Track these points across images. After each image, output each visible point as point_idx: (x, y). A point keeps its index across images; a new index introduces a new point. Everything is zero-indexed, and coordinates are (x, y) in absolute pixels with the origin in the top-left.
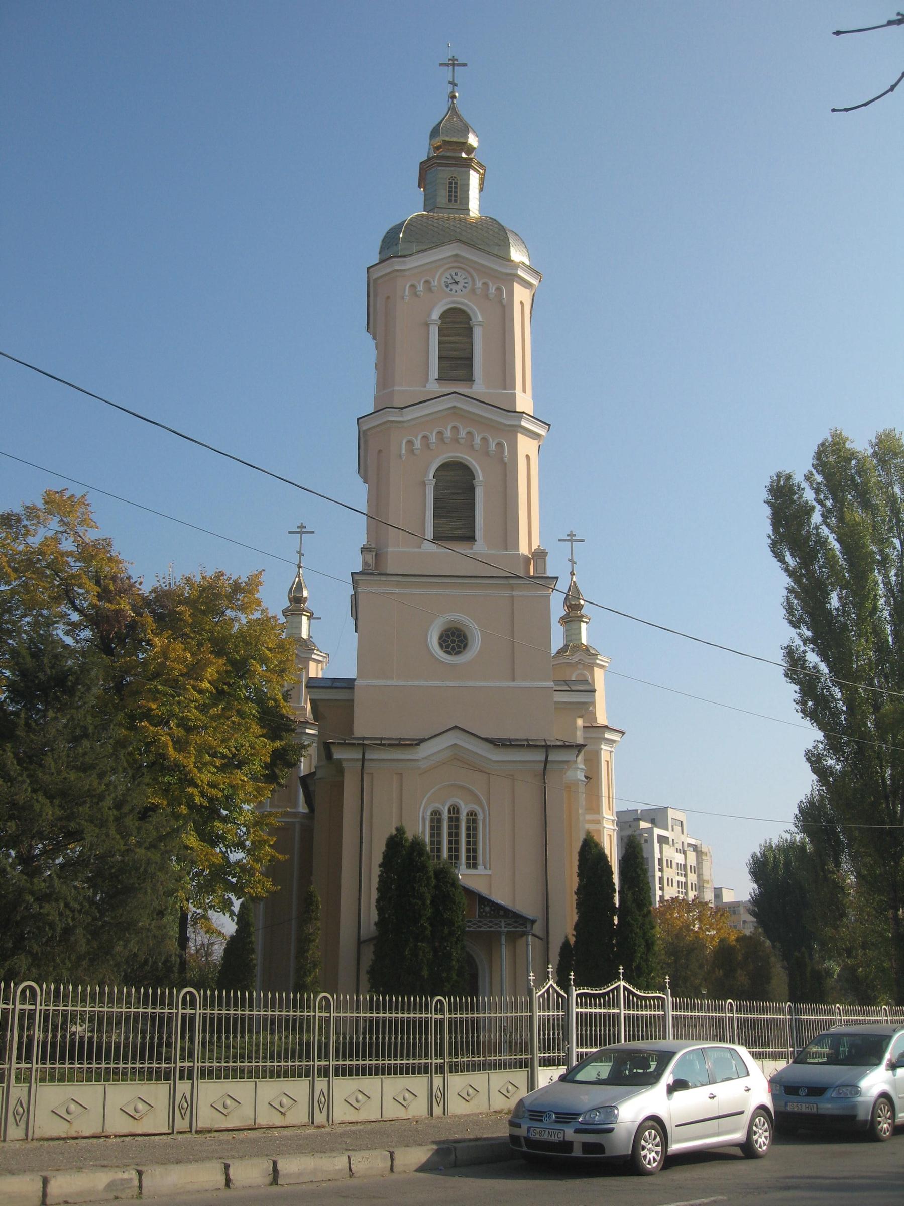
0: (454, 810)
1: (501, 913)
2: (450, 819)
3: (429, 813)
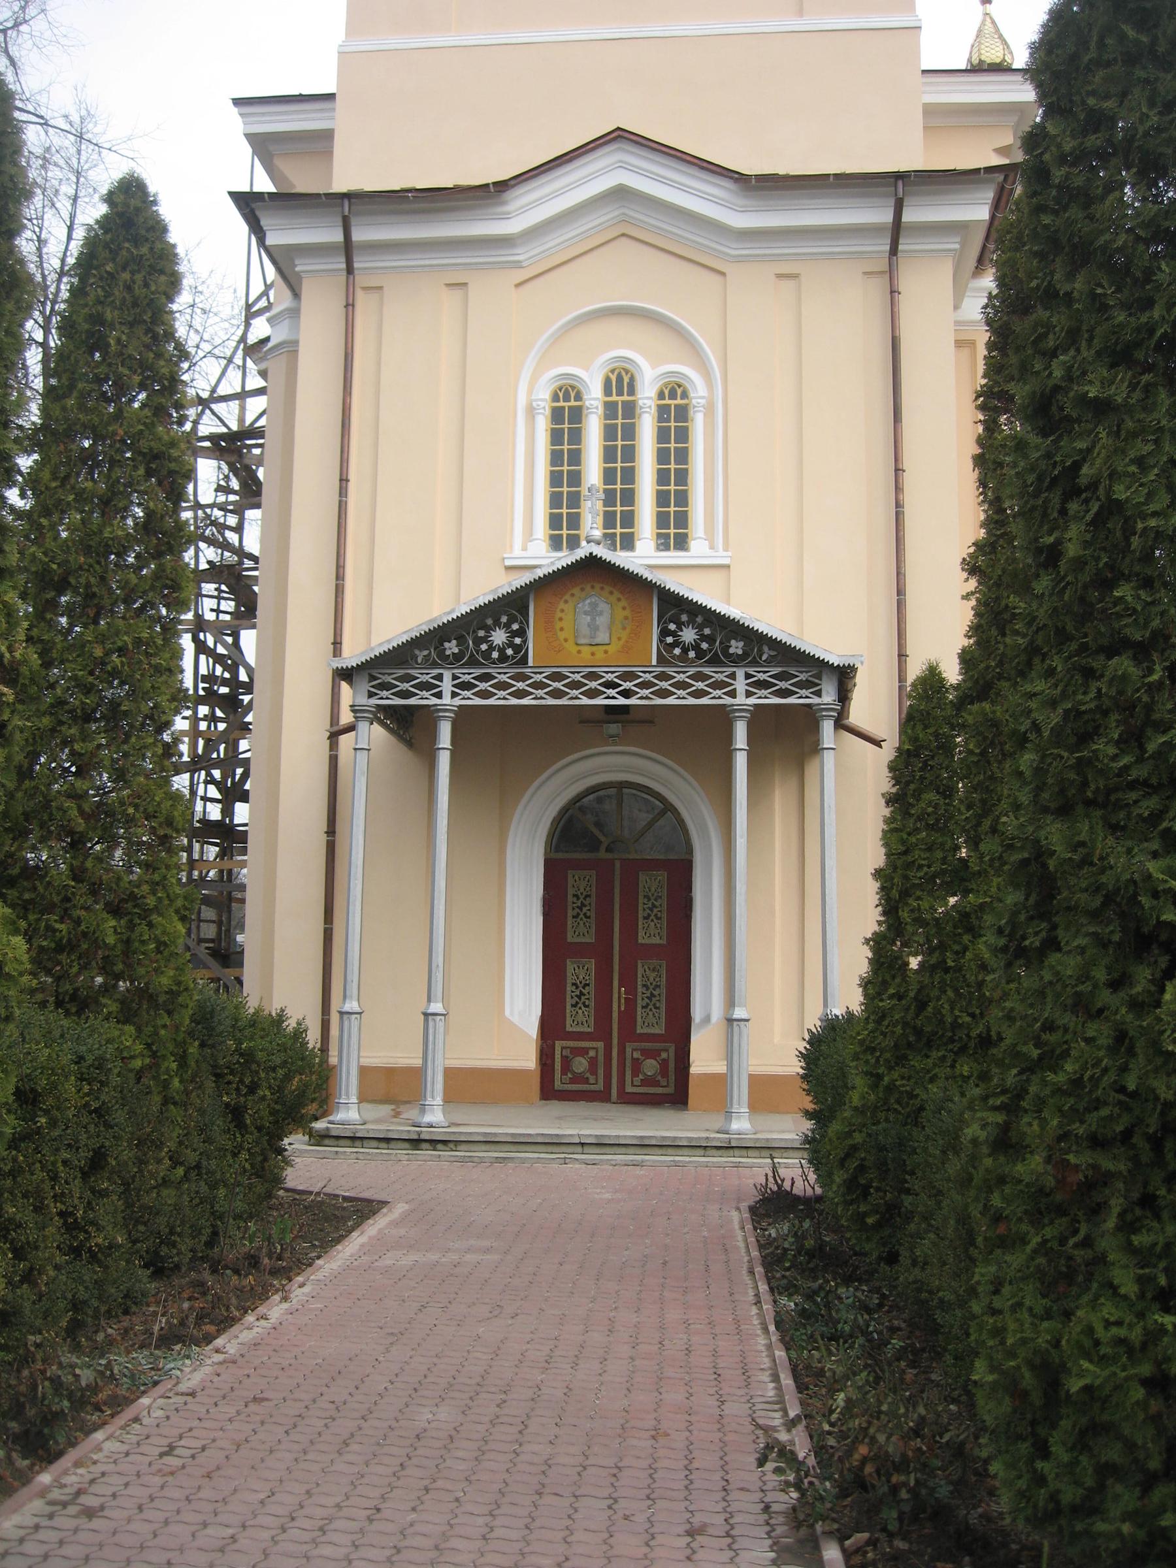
0: (621, 382)
1: (736, 647)
2: (610, 409)
3: (543, 395)
